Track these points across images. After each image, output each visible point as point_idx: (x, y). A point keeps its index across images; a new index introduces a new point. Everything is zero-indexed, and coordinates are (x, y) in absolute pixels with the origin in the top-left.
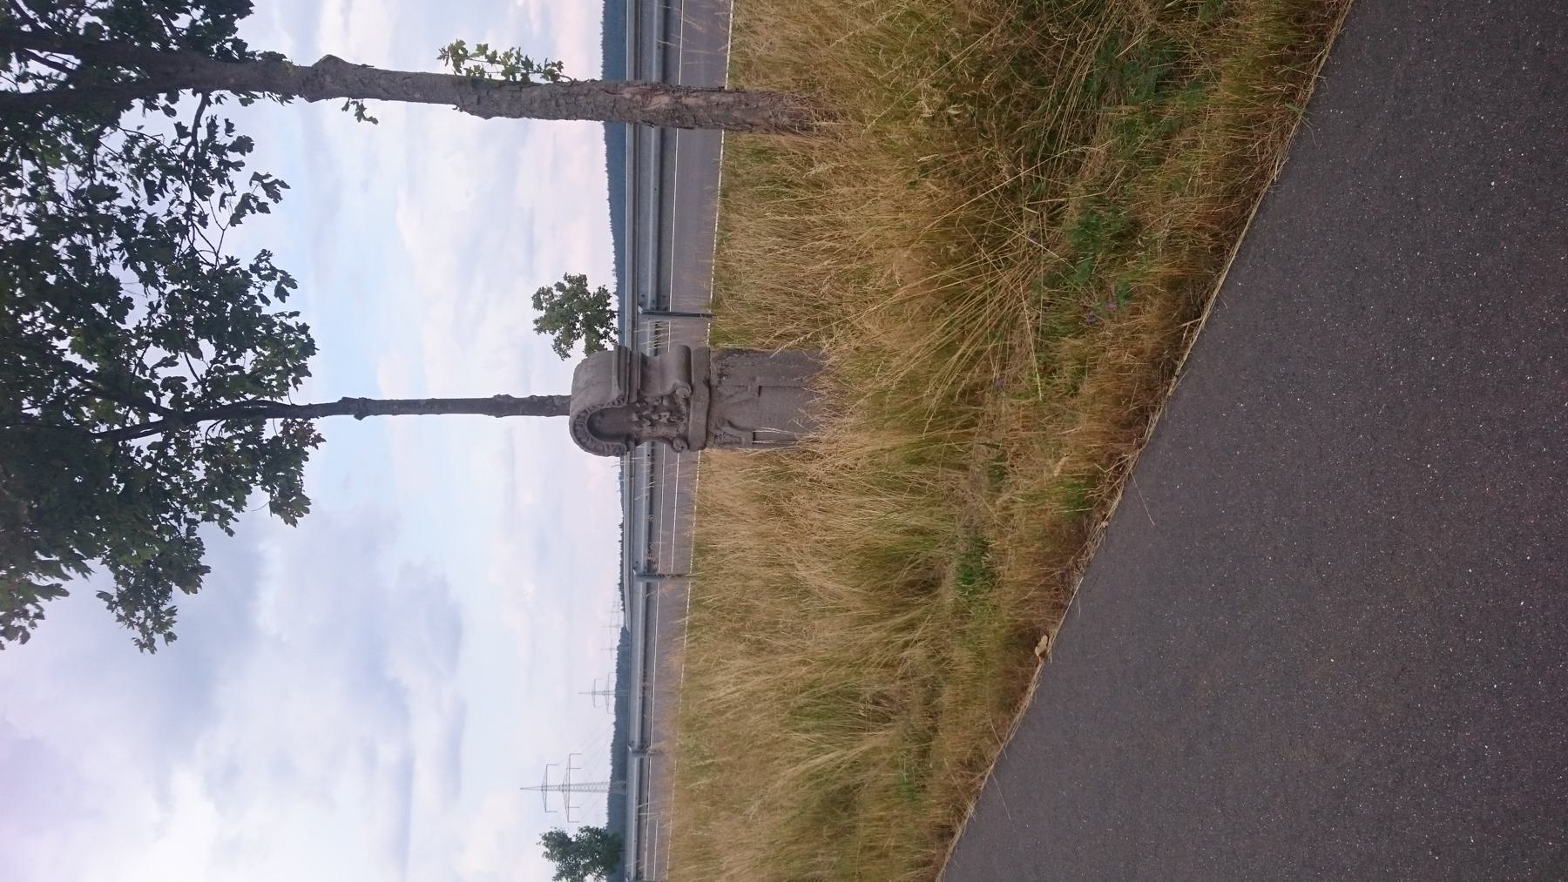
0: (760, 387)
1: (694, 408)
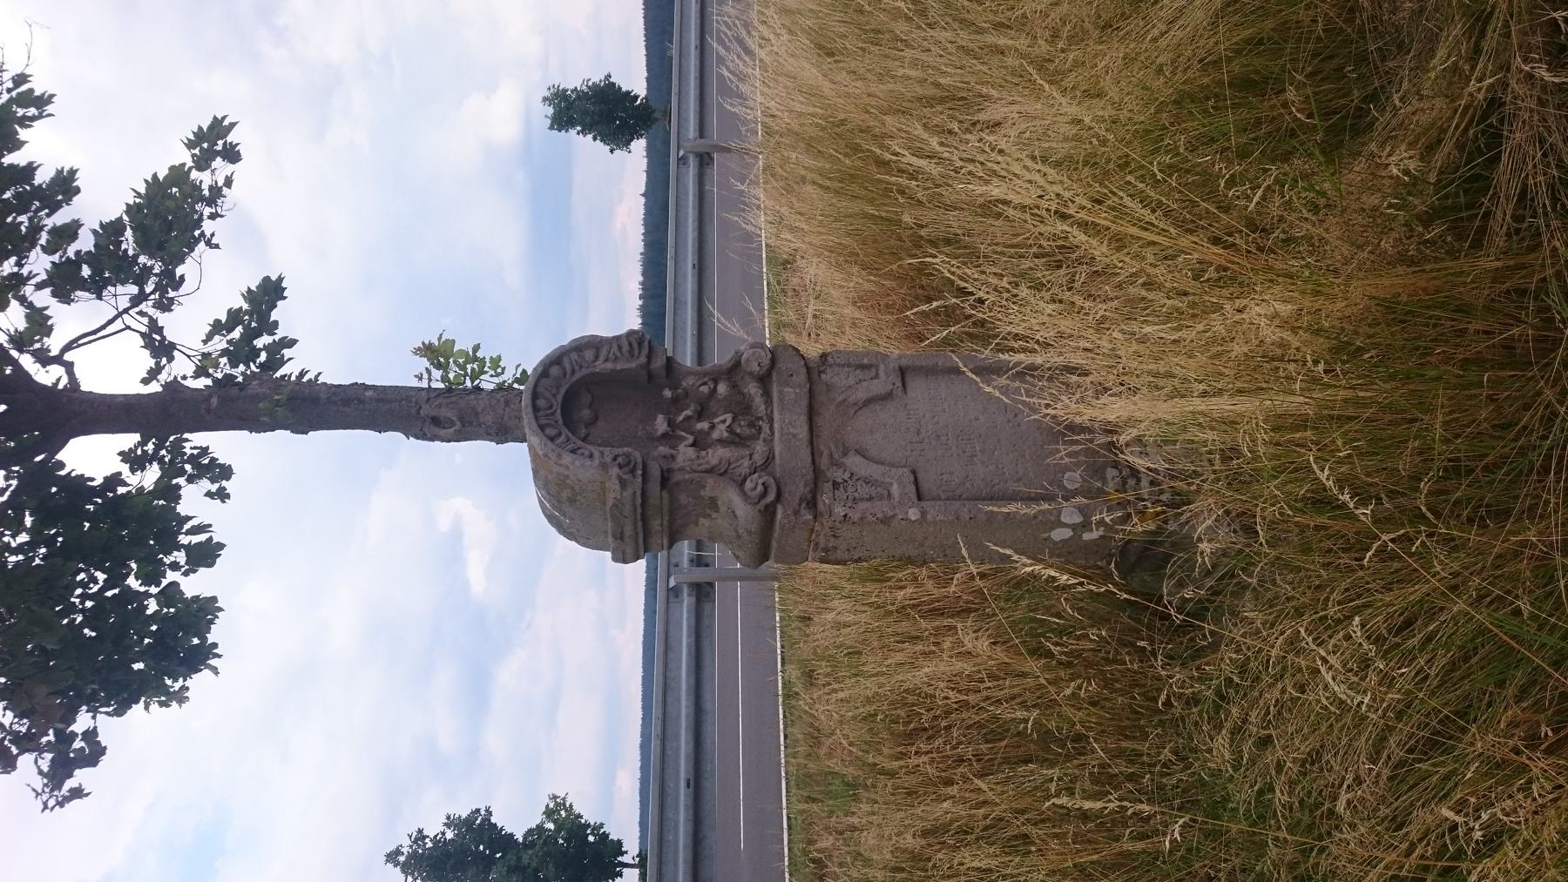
1: (781, 400)
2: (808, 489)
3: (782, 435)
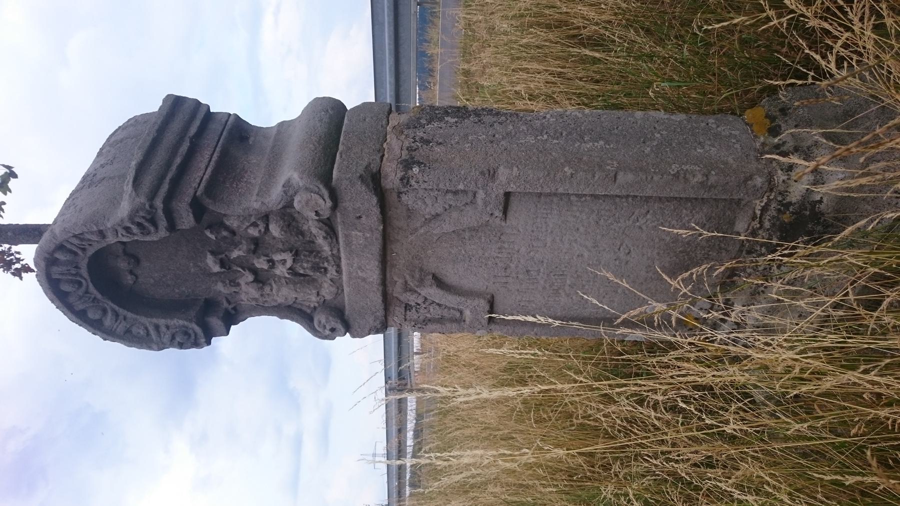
0: (507, 195)
1: (348, 244)
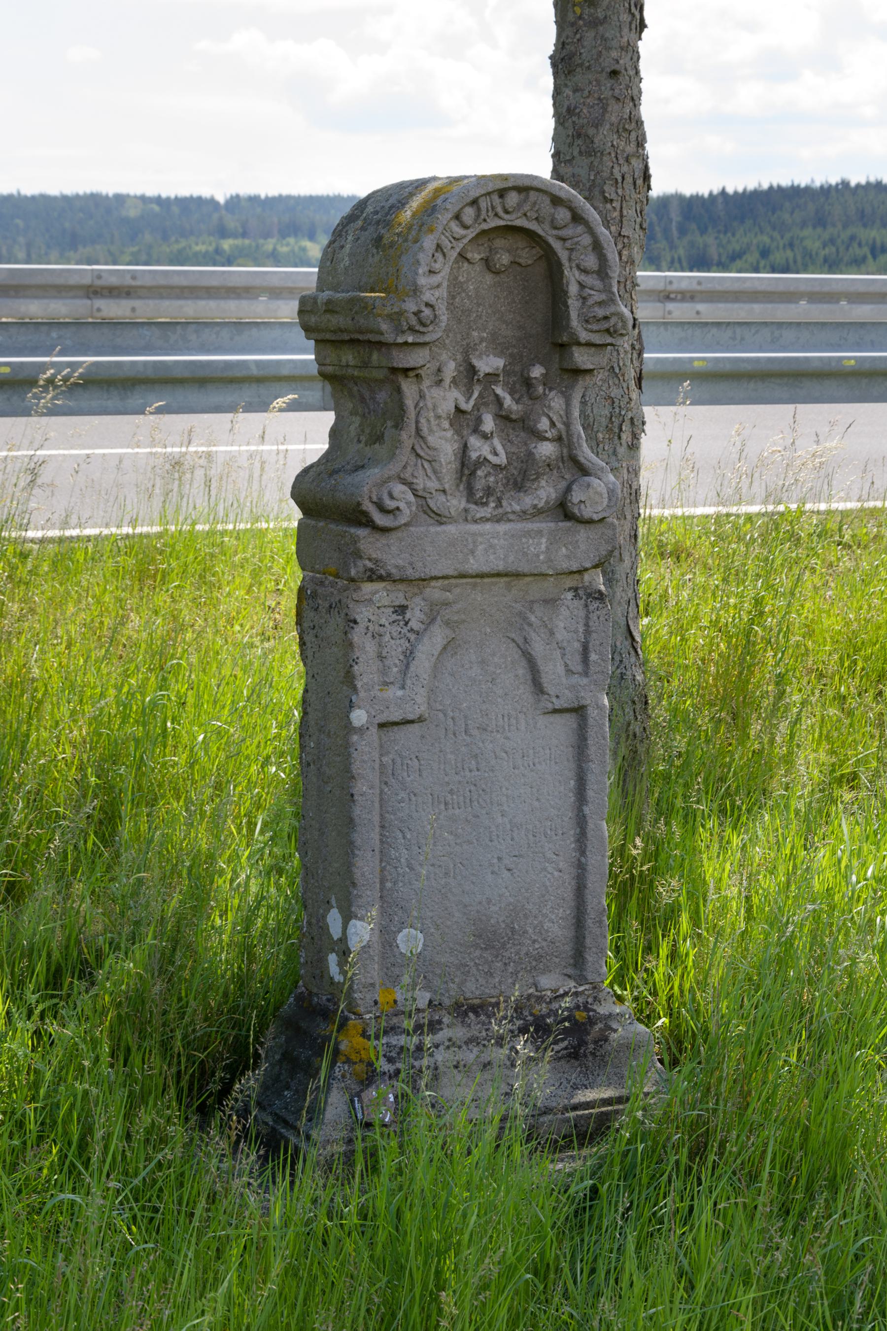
1: (528, 534)
2: (394, 571)
3: (474, 534)
